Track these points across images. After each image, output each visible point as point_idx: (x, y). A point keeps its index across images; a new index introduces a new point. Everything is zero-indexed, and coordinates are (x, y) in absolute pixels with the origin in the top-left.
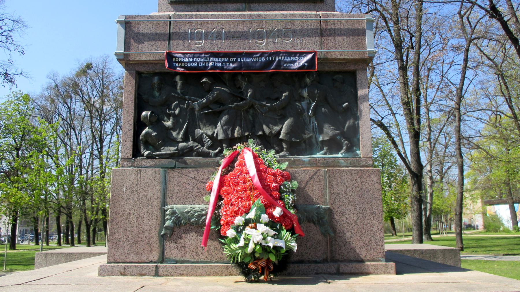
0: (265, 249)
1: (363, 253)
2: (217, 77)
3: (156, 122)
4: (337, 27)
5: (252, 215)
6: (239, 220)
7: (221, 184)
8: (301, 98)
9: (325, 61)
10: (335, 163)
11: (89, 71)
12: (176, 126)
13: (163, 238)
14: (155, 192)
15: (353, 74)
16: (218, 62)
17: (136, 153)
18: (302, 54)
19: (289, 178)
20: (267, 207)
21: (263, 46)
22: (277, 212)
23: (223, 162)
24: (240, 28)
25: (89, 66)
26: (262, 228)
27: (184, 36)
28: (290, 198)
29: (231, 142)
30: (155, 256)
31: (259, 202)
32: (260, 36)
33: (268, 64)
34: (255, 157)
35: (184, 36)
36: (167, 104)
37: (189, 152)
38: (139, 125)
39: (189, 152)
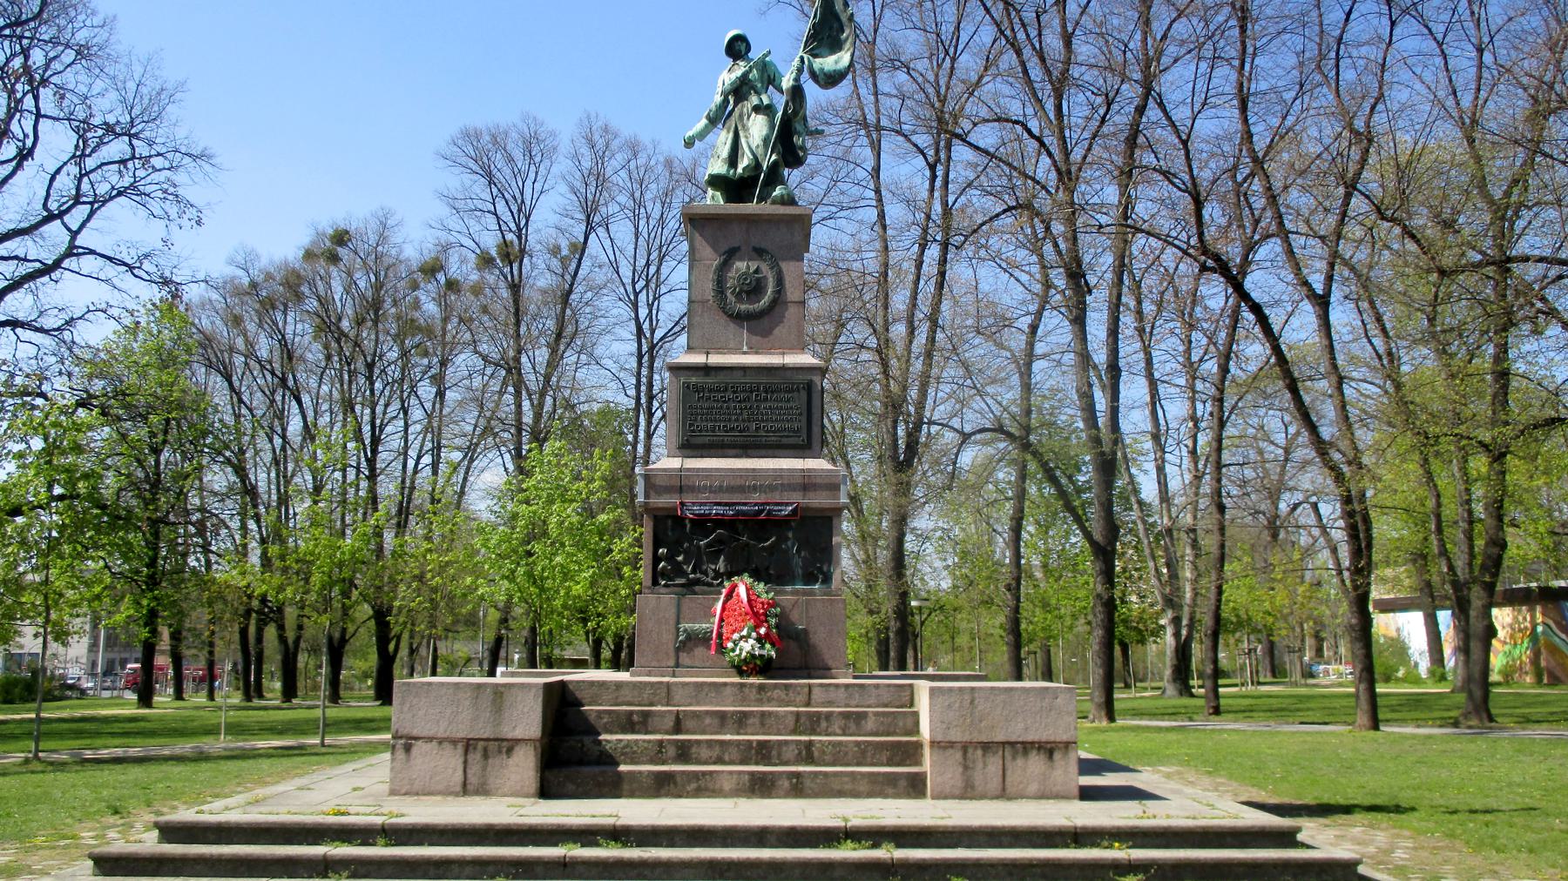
0: (753, 656)
1: (830, 663)
2: (719, 522)
3: (670, 558)
4: (819, 481)
5: (744, 633)
6: (736, 636)
7: (723, 609)
8: (787, 539)
9: (807, 509)
10: (812, 593)
11: (342, 252)
12: (687, 562)
13: (678, 650)
14: (671, 613)
15: (830, 519)
16: (721, 509)
17: (655, 583)
18: (787, 504)
19: (774, 605)
20: (756, 627)
21: (757, 497)
22: (763, 631)
23: (724, 591)
24: (739, 482)
25: (341, 238)
26: (751, 641)
27: (692, 489)
28: (773, 621)
29: (730, 575)
30: (672, 663)
31: (751, 623)
32: (754, 489)
33: (760, 512)
34: (748, 590)
35: (692, 489)
36: (679, 543)
37: (697, 582)
38: (656, 560)
39: (697, 582)
